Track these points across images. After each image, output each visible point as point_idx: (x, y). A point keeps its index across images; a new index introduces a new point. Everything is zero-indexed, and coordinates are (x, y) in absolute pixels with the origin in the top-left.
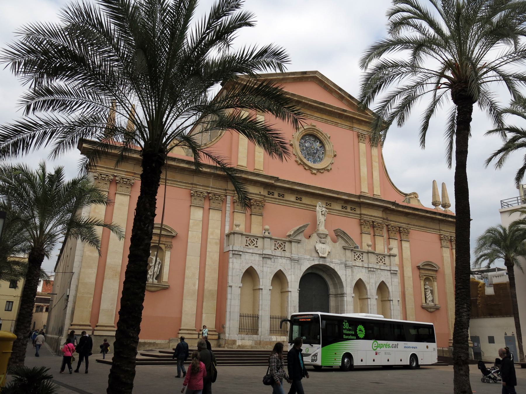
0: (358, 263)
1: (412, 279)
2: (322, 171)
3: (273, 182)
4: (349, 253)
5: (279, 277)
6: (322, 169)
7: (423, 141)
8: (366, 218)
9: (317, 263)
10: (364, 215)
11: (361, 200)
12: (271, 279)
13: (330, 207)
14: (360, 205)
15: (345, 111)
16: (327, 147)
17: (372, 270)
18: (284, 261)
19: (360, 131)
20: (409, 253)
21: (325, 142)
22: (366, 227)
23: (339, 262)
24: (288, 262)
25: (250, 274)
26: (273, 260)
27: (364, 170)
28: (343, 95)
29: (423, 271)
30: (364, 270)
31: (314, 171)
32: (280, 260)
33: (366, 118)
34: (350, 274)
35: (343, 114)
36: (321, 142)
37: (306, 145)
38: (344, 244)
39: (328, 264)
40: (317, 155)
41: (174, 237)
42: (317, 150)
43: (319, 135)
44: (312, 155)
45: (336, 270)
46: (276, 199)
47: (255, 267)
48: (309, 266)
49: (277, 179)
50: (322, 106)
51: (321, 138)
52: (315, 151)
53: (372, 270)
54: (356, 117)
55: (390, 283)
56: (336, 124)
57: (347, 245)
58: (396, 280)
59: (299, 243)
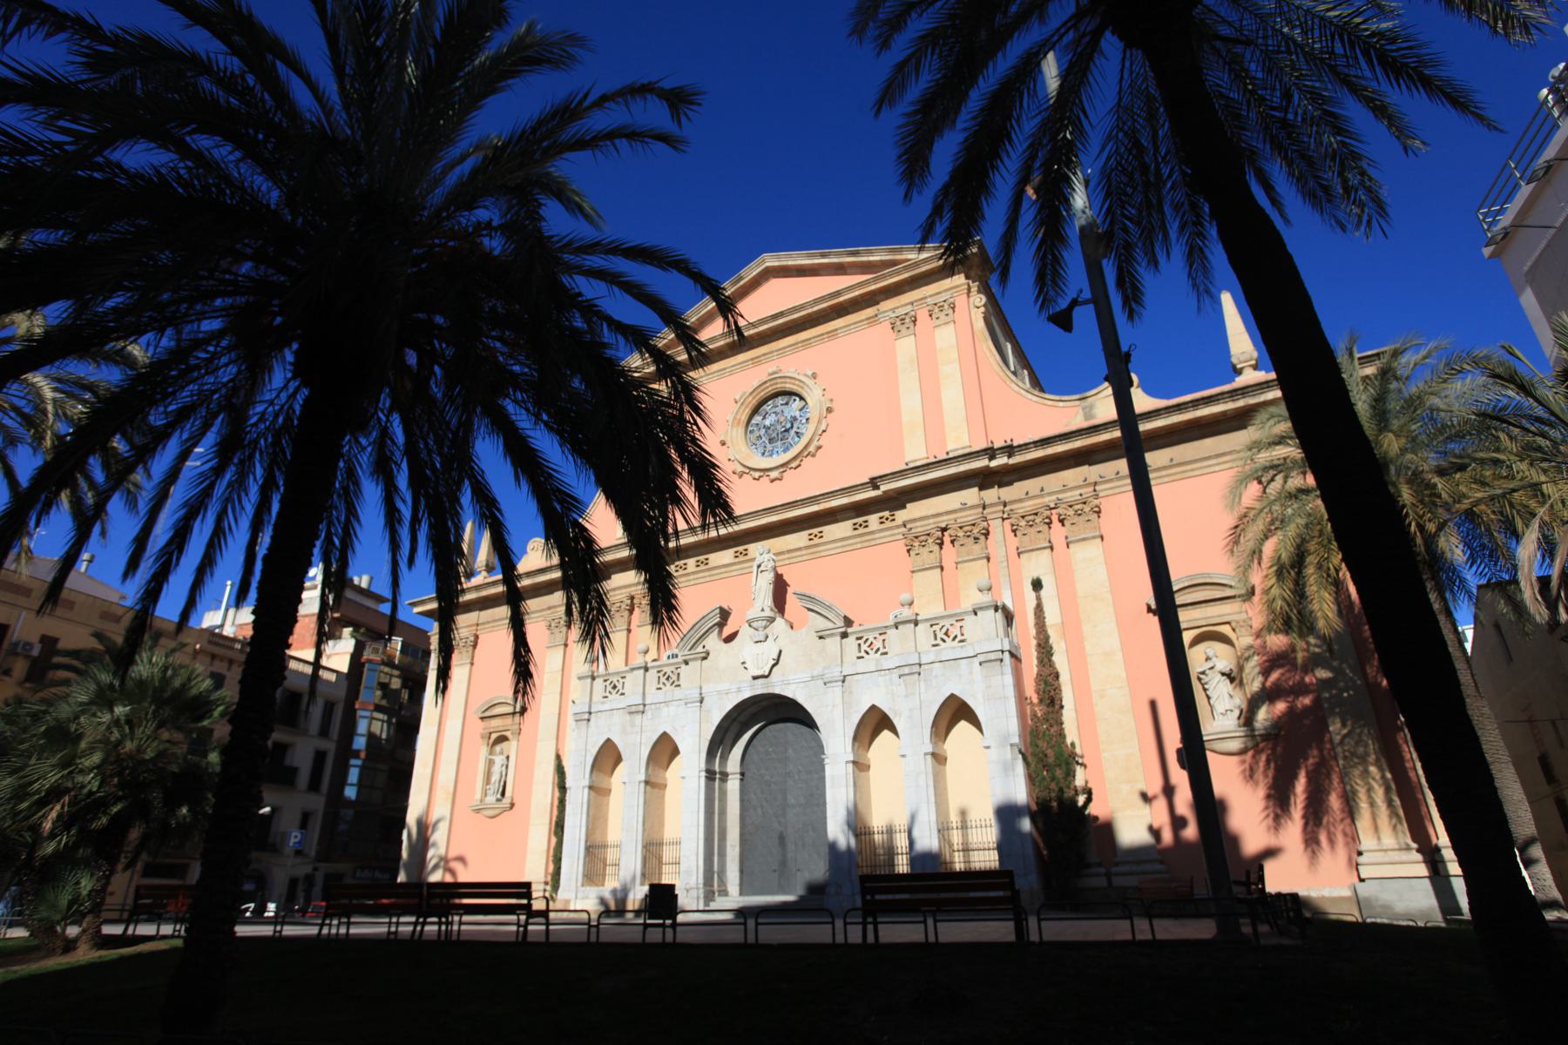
0: (872, 661)
1: (1119, 656)
2: (794, 465)
4: (833, 643)
5: (664, 750)
6: (795, 458)
7: (1490, 126)
8: (919, 528)
9: (747, 694)
11: (884, 488)
15: (838, 293)
17: (906, 670)
18: (672, 709)
20: (1101, 573)
21: (804, 394)
22: (924, 551)
23: (806, 676)
25: (608, 757)
26: (649, 714)
30: (881, 679)
31: (774, 474)
33: (906, 269)
34: (839, 701)
35: (840, 304)
36: (802, 398)
37: (767, 422)
38: (822, 624)
39: (777, 691)
40: (792, 432)
42: (795, 419)
43: (789, 386)
44: (781, 435)
45: (801, 700)
47: (616, 740)
48: (729, 707)
51: (795, 388)
53: (906, 670)
54: (873, 287)
56: (832, 334)
57: (830, 625)
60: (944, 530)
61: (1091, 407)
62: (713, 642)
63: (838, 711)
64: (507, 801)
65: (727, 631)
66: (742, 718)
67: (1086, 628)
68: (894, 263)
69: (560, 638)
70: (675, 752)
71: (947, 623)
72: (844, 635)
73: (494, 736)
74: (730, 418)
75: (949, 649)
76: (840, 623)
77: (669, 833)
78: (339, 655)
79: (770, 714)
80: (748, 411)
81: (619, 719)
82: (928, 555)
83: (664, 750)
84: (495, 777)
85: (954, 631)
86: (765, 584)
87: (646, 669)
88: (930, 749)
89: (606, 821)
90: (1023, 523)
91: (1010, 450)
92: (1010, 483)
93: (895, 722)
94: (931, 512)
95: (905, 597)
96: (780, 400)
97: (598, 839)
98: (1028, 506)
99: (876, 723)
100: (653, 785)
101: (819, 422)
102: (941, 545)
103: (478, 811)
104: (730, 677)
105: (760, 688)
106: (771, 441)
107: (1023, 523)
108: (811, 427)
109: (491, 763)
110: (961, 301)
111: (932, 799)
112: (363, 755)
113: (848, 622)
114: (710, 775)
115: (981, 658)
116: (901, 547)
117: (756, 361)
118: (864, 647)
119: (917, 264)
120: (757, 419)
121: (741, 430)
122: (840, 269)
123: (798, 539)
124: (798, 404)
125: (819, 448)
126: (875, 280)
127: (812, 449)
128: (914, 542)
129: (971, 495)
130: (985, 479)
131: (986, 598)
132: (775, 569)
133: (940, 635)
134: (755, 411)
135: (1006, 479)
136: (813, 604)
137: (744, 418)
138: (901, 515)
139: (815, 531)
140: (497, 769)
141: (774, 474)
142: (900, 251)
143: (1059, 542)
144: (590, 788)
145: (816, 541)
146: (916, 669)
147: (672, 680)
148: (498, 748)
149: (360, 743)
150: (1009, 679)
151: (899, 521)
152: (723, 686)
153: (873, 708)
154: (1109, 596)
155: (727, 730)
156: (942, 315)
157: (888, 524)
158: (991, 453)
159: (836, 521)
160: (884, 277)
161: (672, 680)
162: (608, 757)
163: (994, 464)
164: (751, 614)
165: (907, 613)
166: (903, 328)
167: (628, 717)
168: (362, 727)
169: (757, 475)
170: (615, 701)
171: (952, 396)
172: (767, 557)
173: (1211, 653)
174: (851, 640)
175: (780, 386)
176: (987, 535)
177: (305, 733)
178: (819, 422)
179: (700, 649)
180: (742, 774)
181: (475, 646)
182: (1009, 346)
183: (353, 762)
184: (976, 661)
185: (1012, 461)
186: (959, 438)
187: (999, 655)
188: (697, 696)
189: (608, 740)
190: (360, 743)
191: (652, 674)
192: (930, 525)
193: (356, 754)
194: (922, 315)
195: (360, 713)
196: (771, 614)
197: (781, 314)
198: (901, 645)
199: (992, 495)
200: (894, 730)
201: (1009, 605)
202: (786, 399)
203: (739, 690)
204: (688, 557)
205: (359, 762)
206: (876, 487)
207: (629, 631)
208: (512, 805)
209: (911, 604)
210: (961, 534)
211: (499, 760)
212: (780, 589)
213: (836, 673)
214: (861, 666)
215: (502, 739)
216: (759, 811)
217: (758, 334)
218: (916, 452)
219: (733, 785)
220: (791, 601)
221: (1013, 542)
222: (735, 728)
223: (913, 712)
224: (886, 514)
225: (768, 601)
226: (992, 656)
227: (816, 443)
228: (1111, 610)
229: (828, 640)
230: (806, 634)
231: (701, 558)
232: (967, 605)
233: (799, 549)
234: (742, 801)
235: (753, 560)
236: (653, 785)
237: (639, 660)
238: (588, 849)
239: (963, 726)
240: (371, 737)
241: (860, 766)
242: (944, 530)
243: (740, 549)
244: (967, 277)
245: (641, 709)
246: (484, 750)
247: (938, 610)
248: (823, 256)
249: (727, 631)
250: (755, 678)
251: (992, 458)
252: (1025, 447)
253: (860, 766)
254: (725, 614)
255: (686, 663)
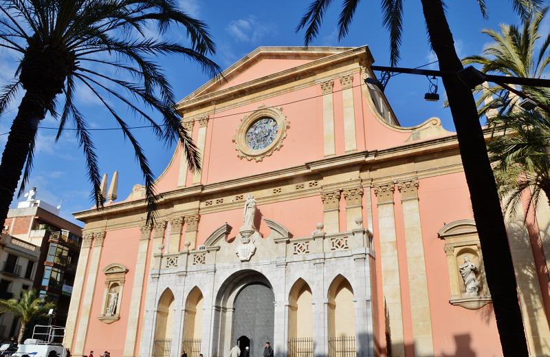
2: (268, 154)
3: (200, 191)
4: (282, 246)
5: (196, 295)
9: (238, 269)
10: (326, 186)
11: (312, 168)
12: (186, 297)
13: (279, 194)
14: (319, 175)
15: (295, 69)
16: (278, 122)
17: (318, 261)
18: (200, 275)
19: (322, 81)
20: (417, 217)
21: (275, 118)
23: (268, 262)
24: (205, 275)
26: (189, 277)
27: (329, 127)
28: (295, 52)
29: (452, 240)
30: (306, 265)
32: (197, 275)
33: (330, 58)
34: (283, 275)
36: (274, 121)
37: (257, 132)
38: (277, 235)
40: (269, 137)
41: (127, 271)
42: (271, 130)
43: (268, 114)
44: (264, 138)
45: (264, 274)
46: (215, 206)
49: (203, 187)
50: (266, 81)
51: (272, 115)
52: (267, 134)
53: (318, 261)
54: (313, 67)
55: (353, 276)
57: (281, 237)
58: (366, 268)
59: (218, 250)
60: (341, 191)
61: (418, 133)
62: (222, 242)
63: (283, 280)
64: (116, 316)
65: (230, 237)
66: (236, 281)
67: (408, 244)
68: (325, 55)
69: (147, 236)
70: (201, 296)
71: (339, 238)
72: (288, 242)
73: (112, 283)
74: (238, 129)
75: (339, 252)
76: (286, 236)
77: (196, 336)
78: (36, 238)
79: (249, 279)
80: (247, 125)
81: (174, 277)
82: (333, 204)
83: (196, 295)
84: (111, 304)
85: (343, 243)
86: (250, 213)
87: (189, 254)
88: (327, 301)
89: (165, 329)
90: (380, 190)
91: (376, 153)
92: (375, 170)
93: (311, 287)
94: (335, 182)
95: (320, 224)
96: (264, 121)
97: (160, 337)
98: (384, 181)
99: (301, 287)
100: (189, 312)
101: (283, 133)
102: (339, 199)
103: (102, 320)
104: (229, 261)
105: (245, 267)
106: (258, 141)
107: (380, 190)
108: (277, 137)
109: (109, 296)
110: (357, 76)
111: (326, 326)
112: (47, 289)
113: (290, 235)
114: (218, 309)
115: (355, 257)
116: (319, 198)
117: (253, 100)
118: (298, 249)
119: (335, 57)
120: (252, 130)
121: (243, 135)
122: (297, 56)
123: (268, 192)
124: (272, 123)
125: (282, 146)
126: (314, 63)
127: (278, 146)
128: (326, 197)
129: (355, 174)
130: (363, 167)
131: (359, 227)
132: (255, 207)
133: (336, 244)
134: (251, 125)
135: (373, 167)
136: (273, 226)
137: (245, 129)
138: (321, 183)
139: (277, 188)
140: (112, 300)
141: (258, 158)
142: (328, 49)
143: (397, 201)
144: (158, 312)
145: (277, 193)
146: (322, 261)
147: (200, 260)
148: (113, 289)
149: (45, 283)
150: (368, 268)
151: (319, 186)
152: (227, 264)
153: (300, 279)
154: (420, 229)
155: (227, 287)
156: (346, 83)
157: (314, 187)
158: (367, 154)
159: (288, 184)
160: (319, 62)
161: (200, 260)
162: (167, 296)
163: (368, 159)
164: (242, 229)
165: (320, 233)
166: (327, 88)
167: (178, 277)
168: (47, 274)
169: (250, 158)
170: (172, 269)
171: (349, 123)
172: (251, 200)
173: (467, 259)
174: (291, 245)
175: (264, 113)
176: (362, 195)
177: (17, 276)
178: (283, 133)
179: (215, 245)
180: (234, 309)
181: (104, 237)
182: (381, 99)
183: (41, 292)
184: (352, 258)
185: (376, 159)
186: (351, 146)
187: (364, 256)
188: (212, 268)
189: (168, 288)
190: (45, 283)
191: (191, 257)
192: (335, 189)
193: (43, 289)
194: (337, 82)
195: (46, 267)
196: (253, 230)
197: (267, 77)
198: (316, 248)
199: (366, 175)
200: (310, 290)
201: (371, 230)
202: (267, 120)
203: (234, 267)
204: (213, 198)
205: (45, 292)
206: (309, 168)
207: (181, 234)
208: (119, 318)
209: (322, 228)
210: (349, 194)
211: (113, 295)
212: (258, 217)
213: (283, 261)
214: (296, 258)
215: (116, 285)
216: (241, 327)
217: (255, 87)
218: (330, 151)
219: (229, 314)
220: (263, 224)
221: (375, 200)
222: (231, 286)
223: (320, 282)
224: (313, 182)
225: (252, 223)
226: (360, 256)
227: (280, 144)
228: (420, 235)
229: (280, 244)
230: (269, 241)
231: (219, 199)
232: (350, 230)
233: (269, 197)
234: (233, 322)
235: (245, 201)
236: (189, 312)
237: (185, 249)
238: (155, 342)
239: (345, 290)
240: (52, 281)
241: (292, 308)
242: (341, 191)
243: (239, 195)
244: (360, 64)
245: (185, 274)
246: (106, 290)
247: (336, 231)
248: (289, 49)
249: (230, 237)
250: (242, 261)
251: (366, 157)
252: (383, 152)
253: (292, 308)
254: (229, 228)
255: (209, 252)
